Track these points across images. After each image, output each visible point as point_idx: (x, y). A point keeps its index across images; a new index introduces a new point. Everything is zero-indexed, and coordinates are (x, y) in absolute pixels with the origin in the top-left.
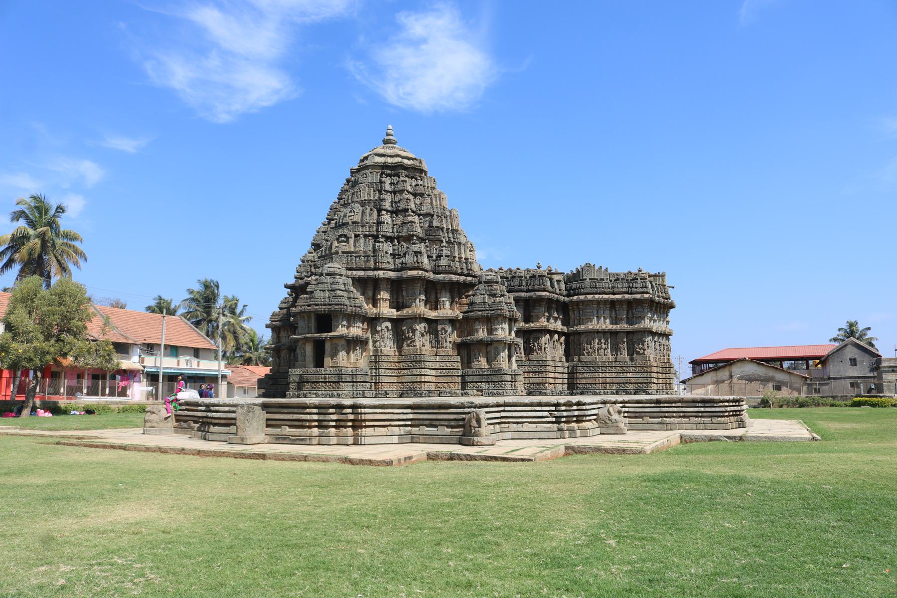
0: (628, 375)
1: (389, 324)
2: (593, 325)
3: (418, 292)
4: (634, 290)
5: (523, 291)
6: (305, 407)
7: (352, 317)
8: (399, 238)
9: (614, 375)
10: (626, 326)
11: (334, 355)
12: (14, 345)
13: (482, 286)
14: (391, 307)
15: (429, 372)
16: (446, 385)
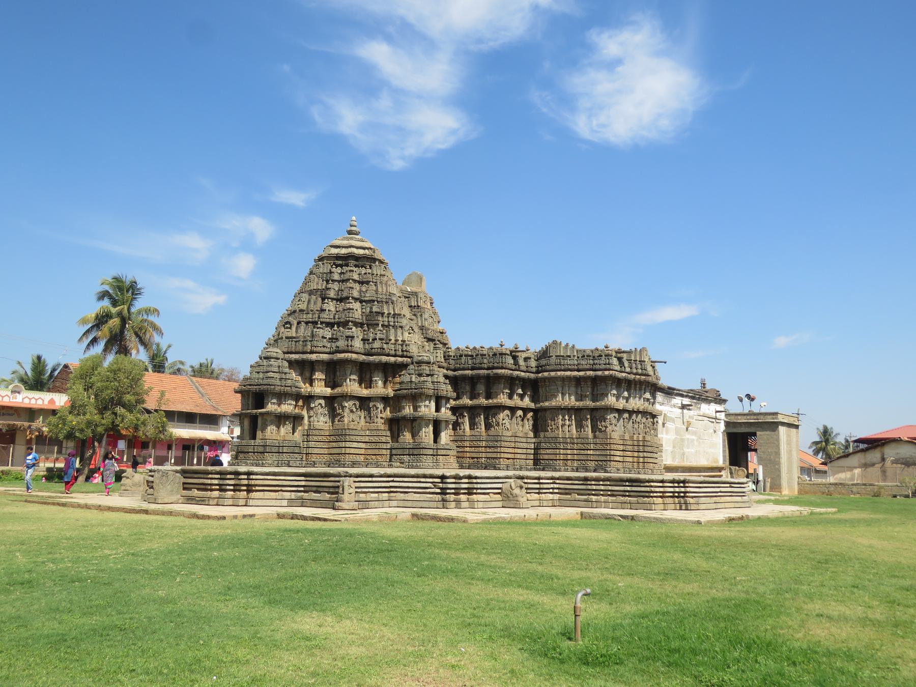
0: (589, 452)
1: (322, 402)
2: (560, 400)
3: (348, 372)
4: (598, 367)
5: (484, 369)
6: (207, 473)
7: (282, 397)
8: (339, 324)
9: (575, 452)
10: (589, 403)
11: (263, 430)
12: (70, 417)
13: (411, 367)
14: (326, 386)
15: (355, 445)
16: (374, 457)
